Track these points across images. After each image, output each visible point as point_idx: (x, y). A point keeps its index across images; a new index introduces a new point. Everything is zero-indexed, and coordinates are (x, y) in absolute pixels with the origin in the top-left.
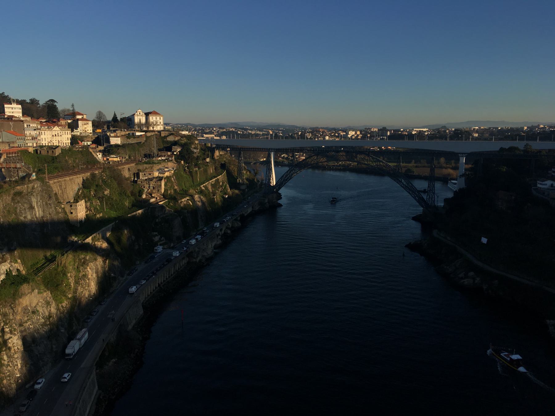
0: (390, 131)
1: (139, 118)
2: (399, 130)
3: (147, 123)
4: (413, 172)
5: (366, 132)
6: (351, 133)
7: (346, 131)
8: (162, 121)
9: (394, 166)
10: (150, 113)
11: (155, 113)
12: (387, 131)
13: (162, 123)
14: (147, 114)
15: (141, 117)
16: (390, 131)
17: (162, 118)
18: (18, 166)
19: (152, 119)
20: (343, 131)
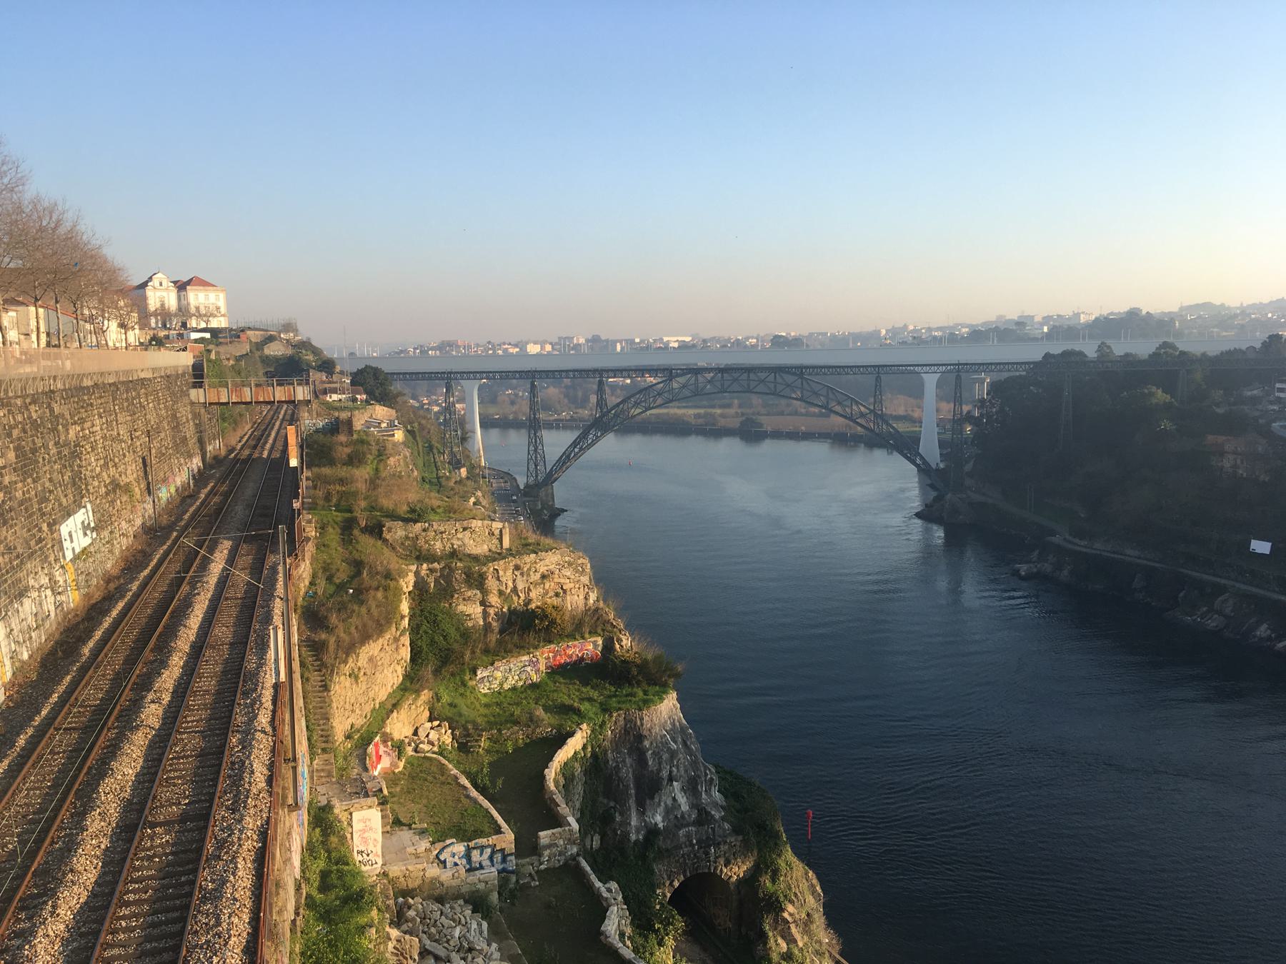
0: (621, 342)
1: (161, 296)
2: (632, 341)
3: (183, 311)
4: (761, 425)
5: (563, 344)
6: (533, 349)
7: (521, 345)
8: (222, 303)
9: (698, 416)
10: (189, 282)
11: (204, 284)
12: (615, 342)
13: (223, 310)
14: (181, 287)
15: (164, 294)
16: (621, 342)
17: (222, 296)
18: (301, 393)
19: (196, 297)
20: (516, 346)
